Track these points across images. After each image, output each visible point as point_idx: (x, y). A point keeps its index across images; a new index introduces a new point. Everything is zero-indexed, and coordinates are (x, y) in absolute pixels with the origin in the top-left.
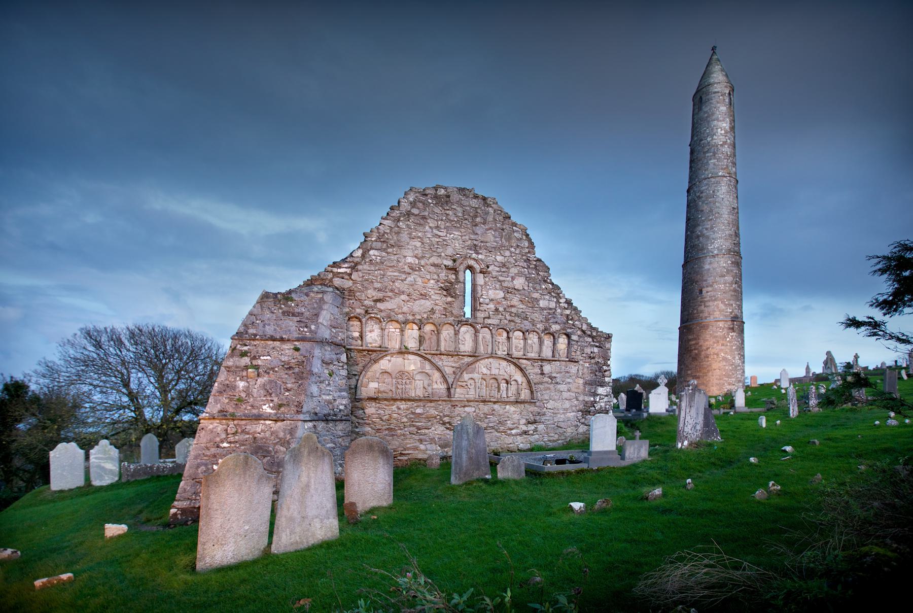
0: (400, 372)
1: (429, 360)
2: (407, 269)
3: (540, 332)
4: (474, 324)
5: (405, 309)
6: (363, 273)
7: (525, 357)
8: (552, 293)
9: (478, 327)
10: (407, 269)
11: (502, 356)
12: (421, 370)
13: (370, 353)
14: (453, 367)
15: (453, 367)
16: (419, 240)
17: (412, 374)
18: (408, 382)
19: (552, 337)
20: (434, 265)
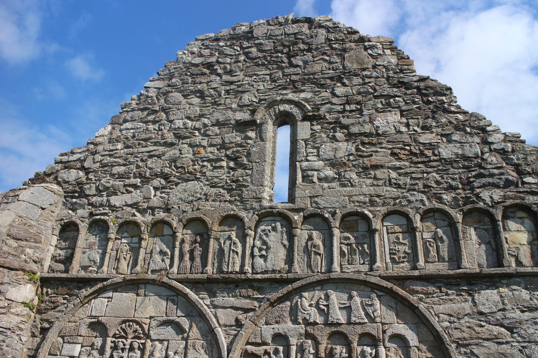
0: (124, 322)
1: (186, 296)
2: (170, 137)
3: (452, 212)
4: (290, 214)
5: (155, 201)
6: (103, 156)
7: (416, 273)
8: (468, 130)
9: (297, 217)
10: (170, 137)
11: (355, 276)
12: (165, 318)
13: (81, 285)
14: (236, 309)
15: (236, 309)
16: (198, 95)
17: (146, 327)
18: (136, 345)
19: (487, 220)
20: (218, 124)
